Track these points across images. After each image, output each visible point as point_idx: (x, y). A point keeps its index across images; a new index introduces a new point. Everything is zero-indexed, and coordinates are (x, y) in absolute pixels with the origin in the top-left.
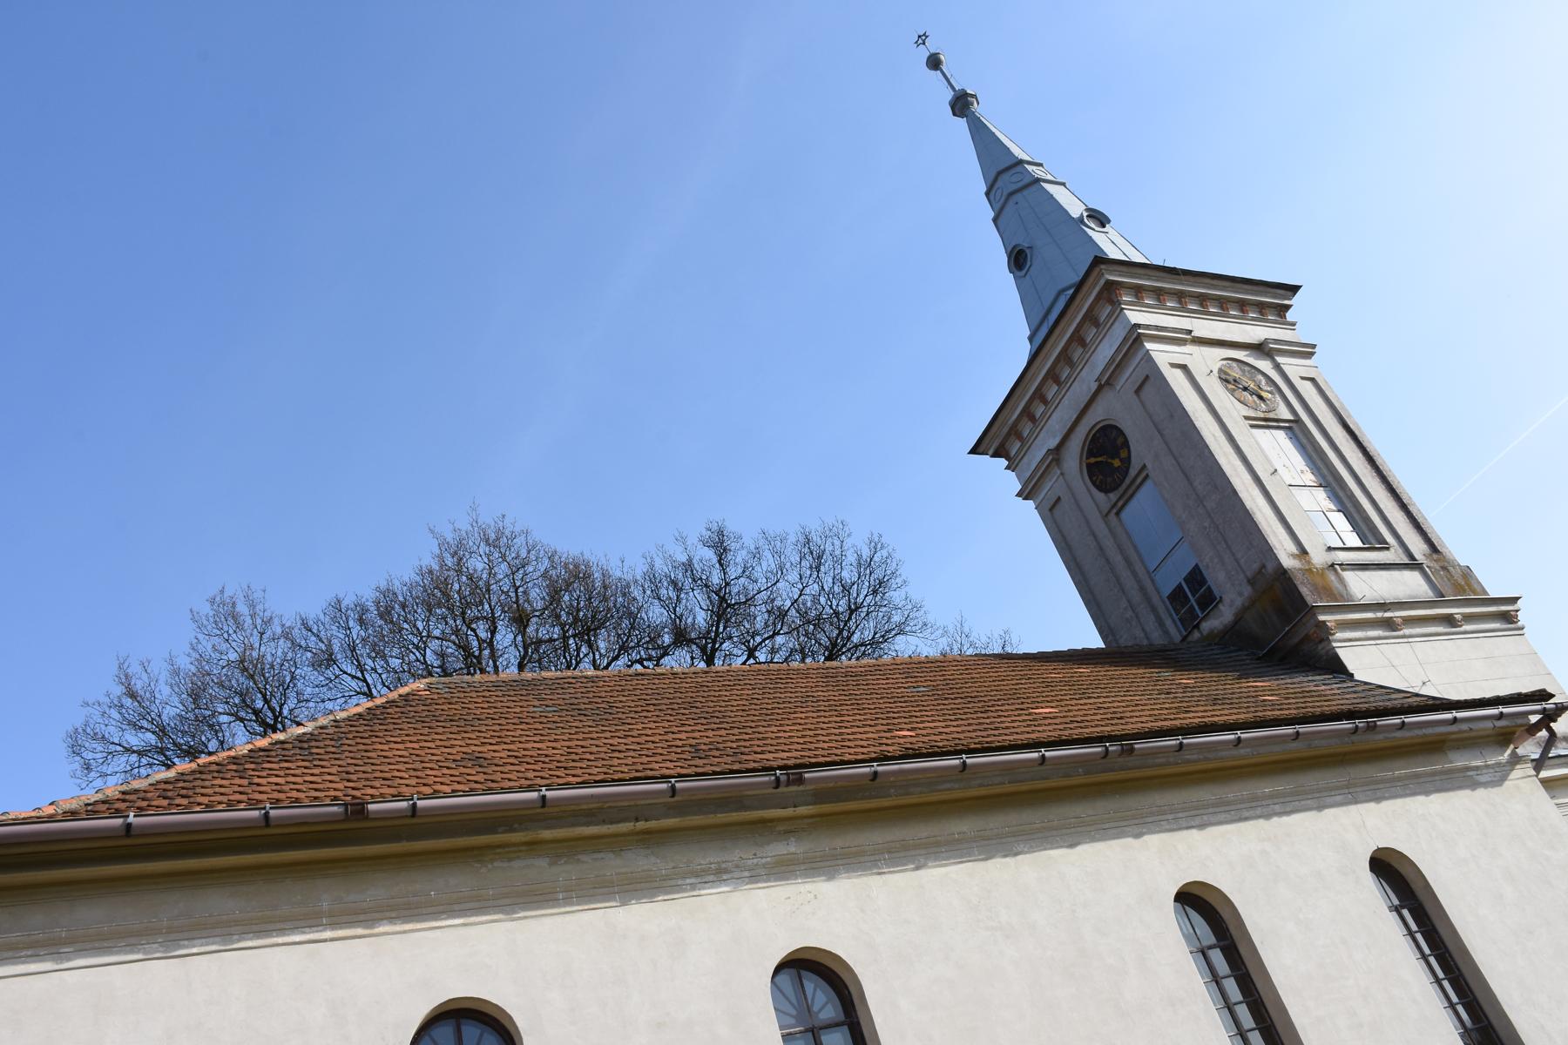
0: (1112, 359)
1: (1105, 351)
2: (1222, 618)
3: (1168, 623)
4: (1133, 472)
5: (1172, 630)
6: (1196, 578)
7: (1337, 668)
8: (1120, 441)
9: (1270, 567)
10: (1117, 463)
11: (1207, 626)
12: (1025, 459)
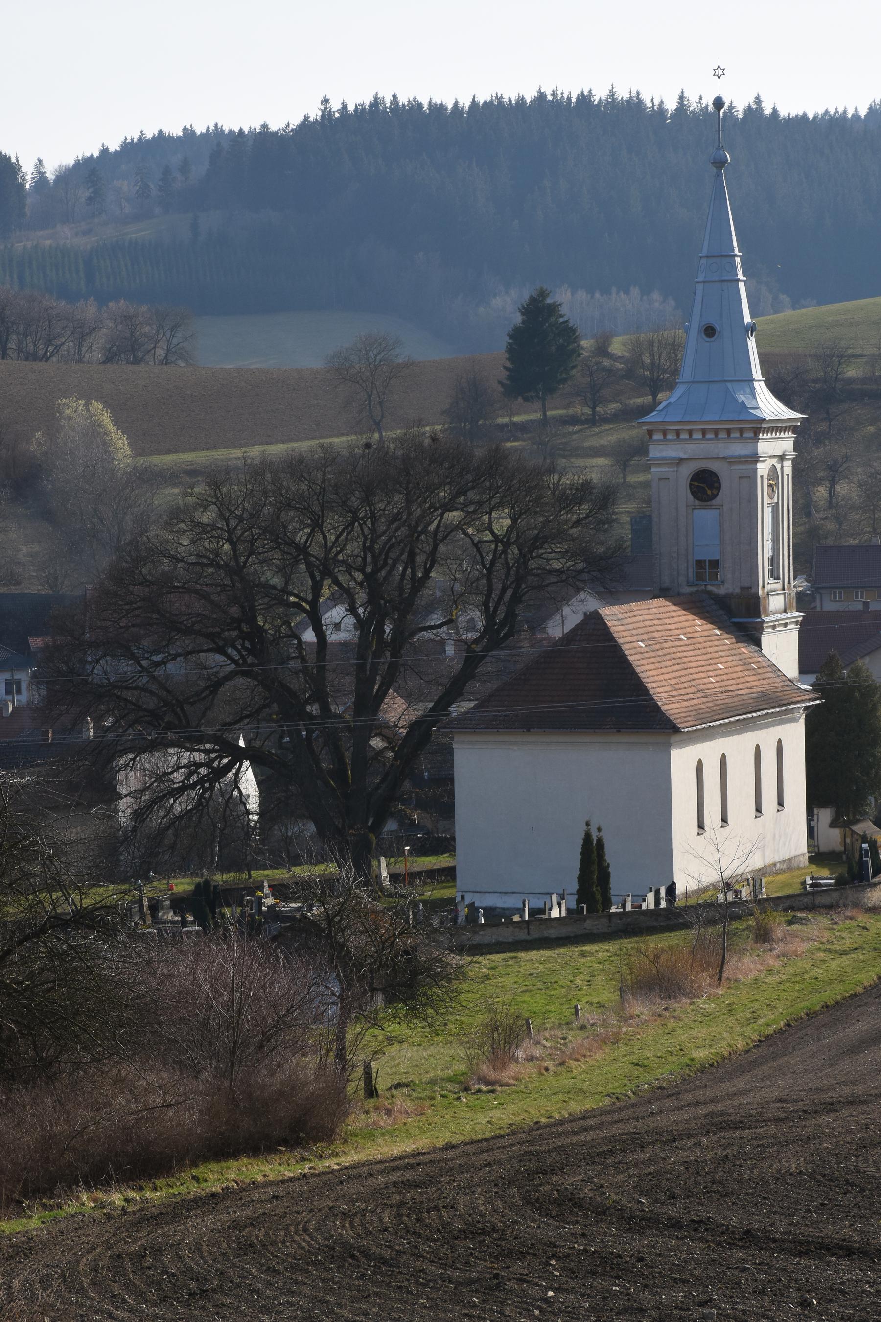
0: (740, 457)
1: (737, 449)
2: (722, 591)
3: (691, 570)
4: (714, 502)
5: (691, 575)
6: (715, 564)
7: (758, 643)
8: (716, 485)
9: (753, 590)
10: (709, 492)
11: (710, 588)
12: (661, 447)
